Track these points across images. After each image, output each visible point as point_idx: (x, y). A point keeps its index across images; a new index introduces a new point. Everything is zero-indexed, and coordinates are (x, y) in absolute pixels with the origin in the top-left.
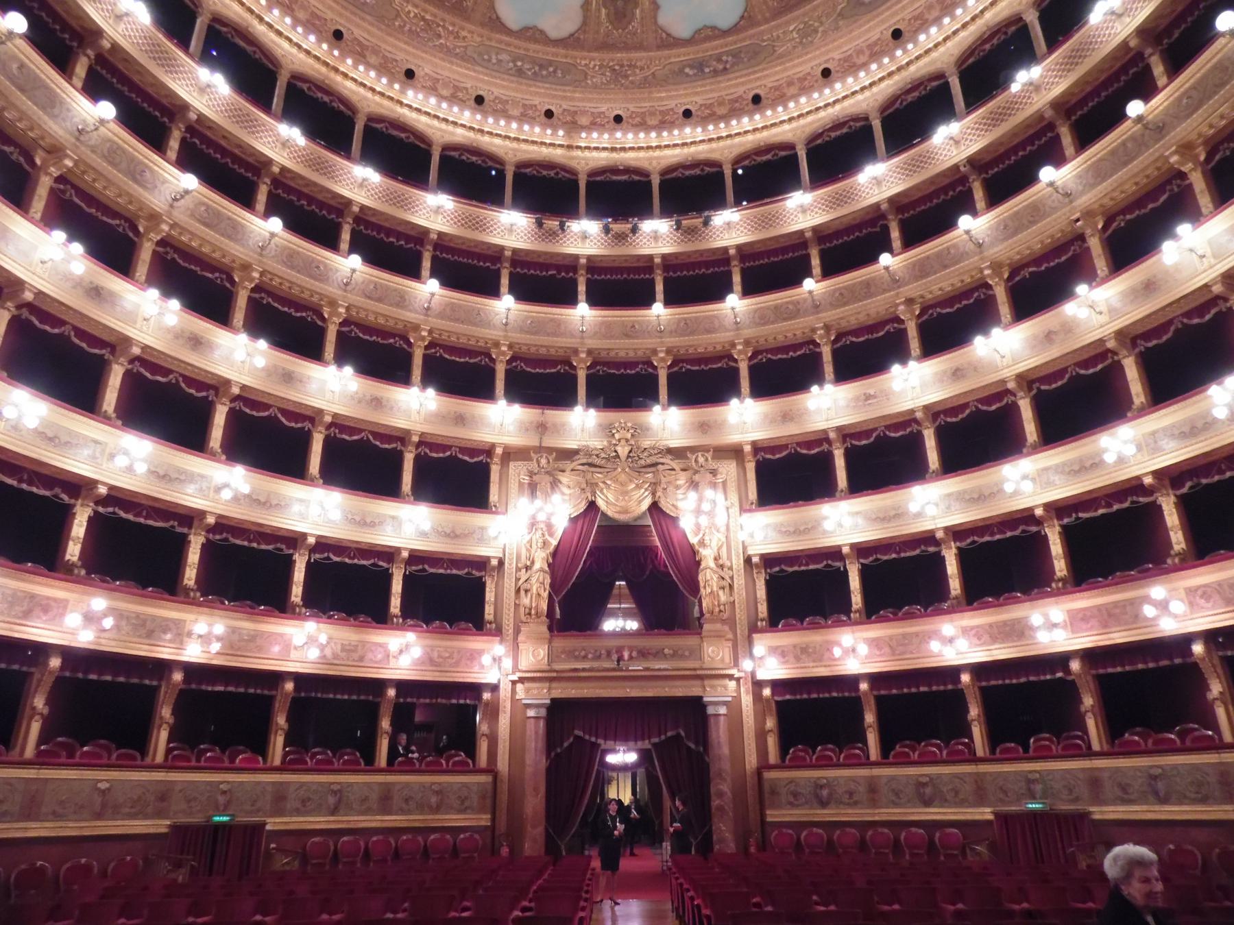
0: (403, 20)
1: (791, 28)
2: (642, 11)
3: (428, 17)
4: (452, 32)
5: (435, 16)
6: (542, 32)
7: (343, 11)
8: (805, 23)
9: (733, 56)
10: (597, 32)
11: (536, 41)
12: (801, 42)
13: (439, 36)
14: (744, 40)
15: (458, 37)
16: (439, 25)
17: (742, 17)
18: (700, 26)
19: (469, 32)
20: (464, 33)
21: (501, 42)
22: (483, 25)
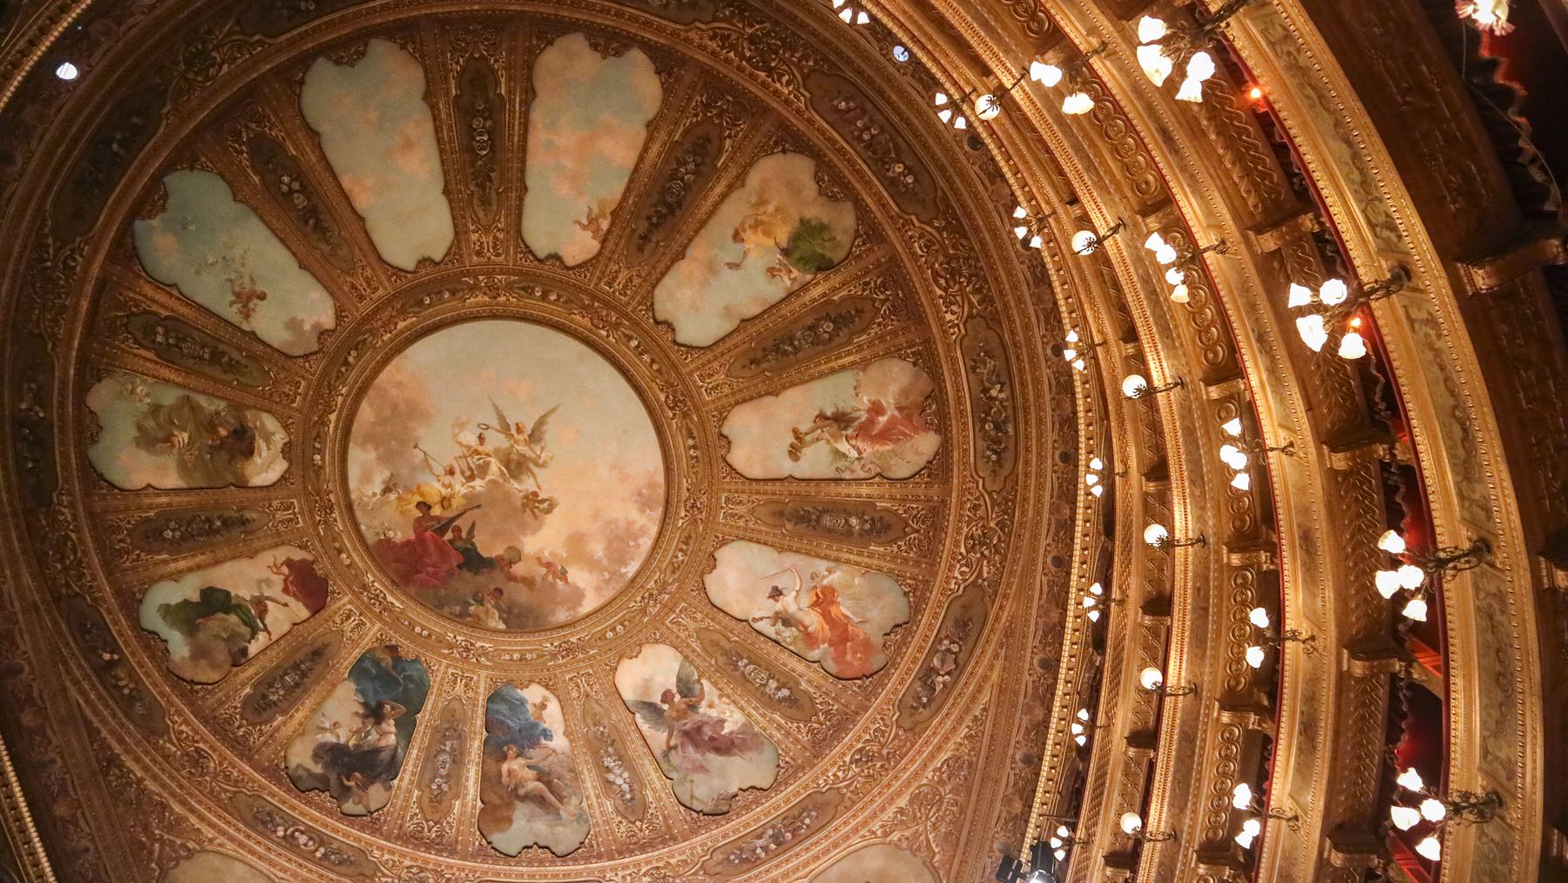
0: (801, 70)
1: (225, 68)
2: (447, 92)
3: (763, 74)
4: (732, 47)
5: (751, 75)
6: (594, 47)
7: (884, 85)
8: (208, 78)
9: (299, 10)
10: (511, 51)
11: (603, 30)
12: (204, 42)
13: (752, 40)
14: (292, 42)
15: (725, 38)
16: (749, 60)
17: (302, 83)
18: (360, 65)
19: (702, 47)
20: (713, 45)
21: (660, 30)
22: (684, 61)
